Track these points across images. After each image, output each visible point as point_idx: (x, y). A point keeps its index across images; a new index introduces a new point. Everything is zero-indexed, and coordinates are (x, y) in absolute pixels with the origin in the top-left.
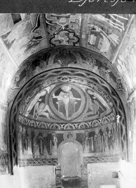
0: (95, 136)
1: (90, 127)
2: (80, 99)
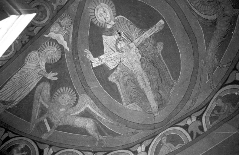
2: (161, 22)
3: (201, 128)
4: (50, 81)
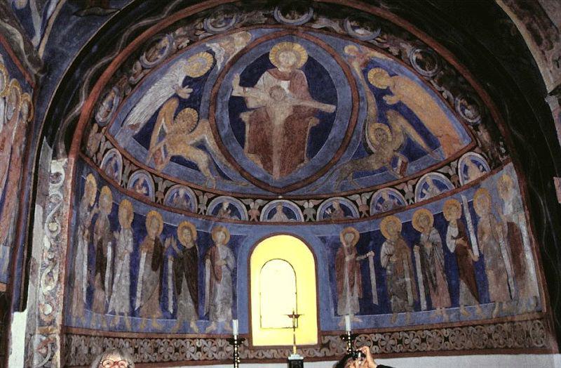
0: (385, 249)
1: (361, 213)
3: (315, 216)
4: (180, 98)
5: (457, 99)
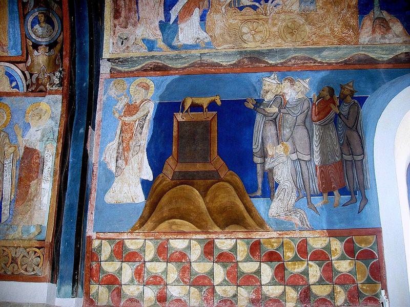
5: (36, 10)
